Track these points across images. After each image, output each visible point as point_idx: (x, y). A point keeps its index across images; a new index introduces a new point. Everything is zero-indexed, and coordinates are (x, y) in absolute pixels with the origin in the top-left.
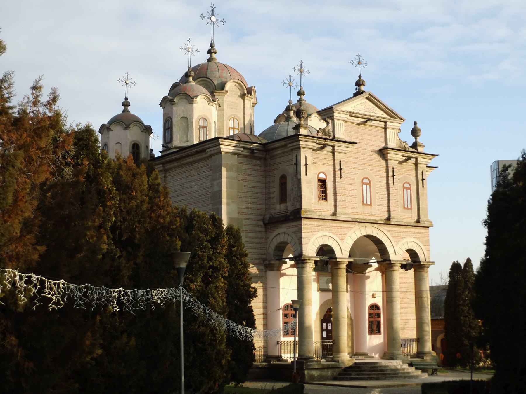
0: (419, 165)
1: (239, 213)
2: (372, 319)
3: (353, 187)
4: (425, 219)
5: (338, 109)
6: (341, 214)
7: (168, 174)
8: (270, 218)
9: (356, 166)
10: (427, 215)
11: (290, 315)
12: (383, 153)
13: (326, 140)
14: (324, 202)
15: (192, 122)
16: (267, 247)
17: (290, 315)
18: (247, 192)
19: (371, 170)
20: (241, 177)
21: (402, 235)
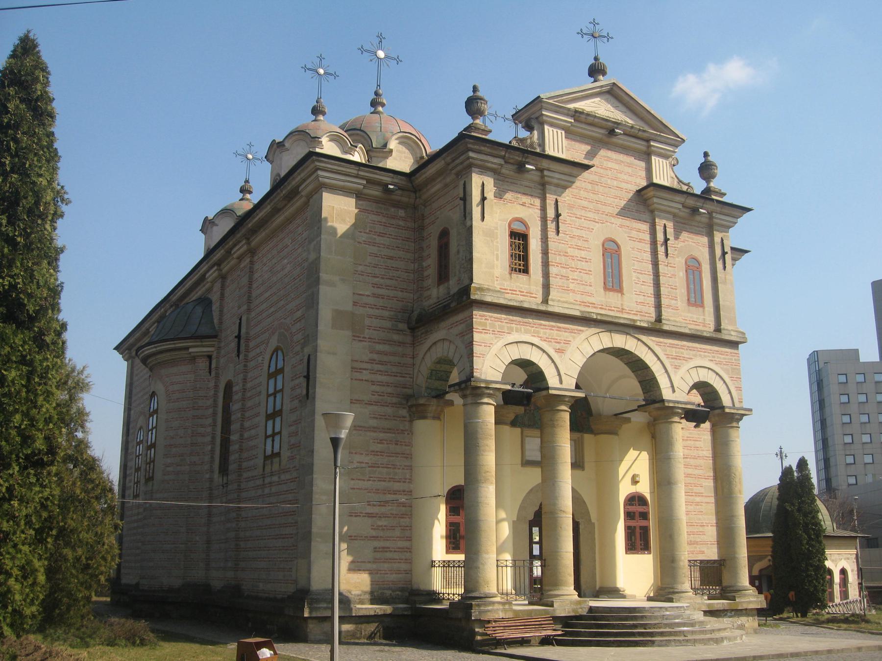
0: (715, 227)
1: (355, 304)
2: (632, 523)
3: (583, 254)
4: (730, 328)
7: (256, 257)
9: (590, 215)
10: (733, 321)
14: (522, 277)
16: (416, 371)
19: (621, 226)
20: (364, 237)
21: (686, 353)
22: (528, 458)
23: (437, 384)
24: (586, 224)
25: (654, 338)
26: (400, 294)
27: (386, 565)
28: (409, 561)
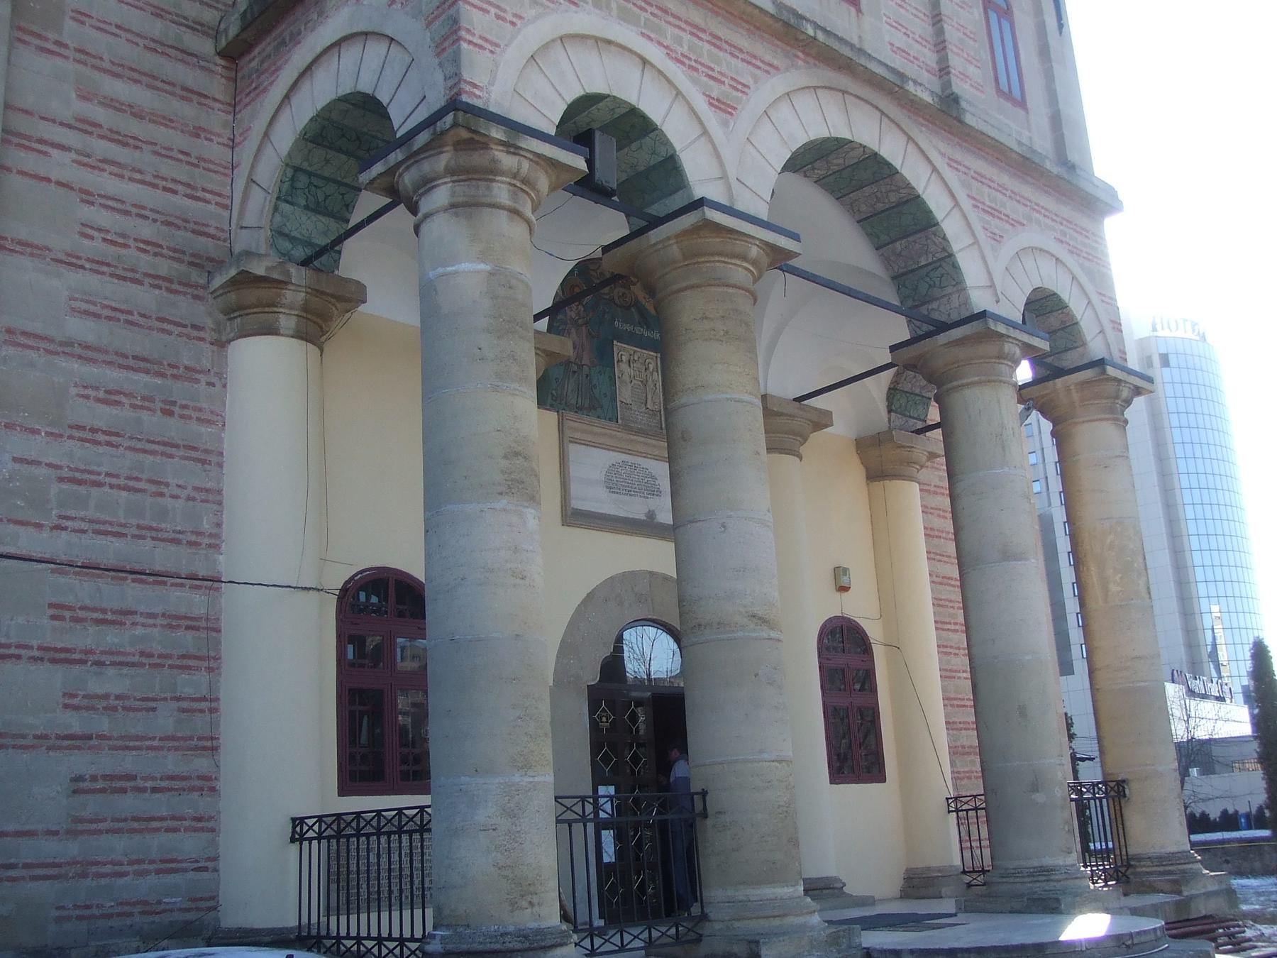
16: (240, 184)
21: (1010, 207)
22: (576, 504)
25: (943, 146)
27: (119, 845)
28: (206, 824)
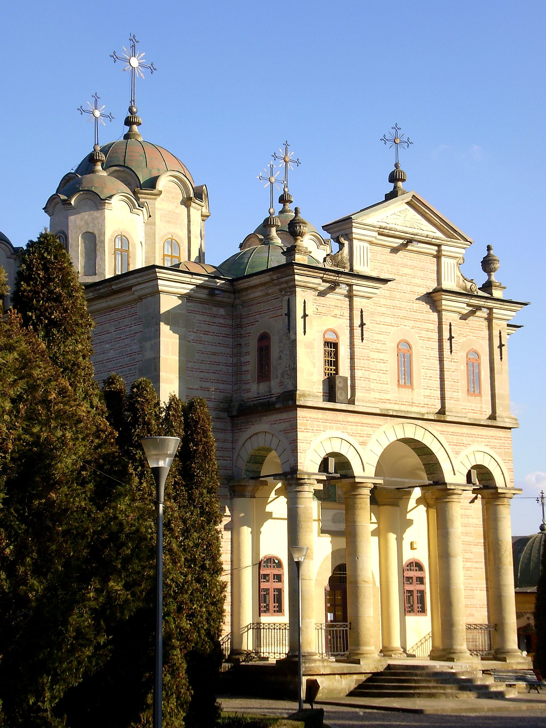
0: (495, 321)
3: (382, 356)
4: (504, 414)
5: (359, 220)
6: (363, 401)
8: (240, 406)
9: (388, 320)
11: (271, 577)
12: (432, 299)
13: (339, 275)
15: (103, 242)
16: (235, 455)
17: (271, 577)
18: (202, 362)
19: (413, 327)
21: (465, 440)
23: (254, 467)
24: (384, 328)
25: (438, 428)
26: (222, 386)
